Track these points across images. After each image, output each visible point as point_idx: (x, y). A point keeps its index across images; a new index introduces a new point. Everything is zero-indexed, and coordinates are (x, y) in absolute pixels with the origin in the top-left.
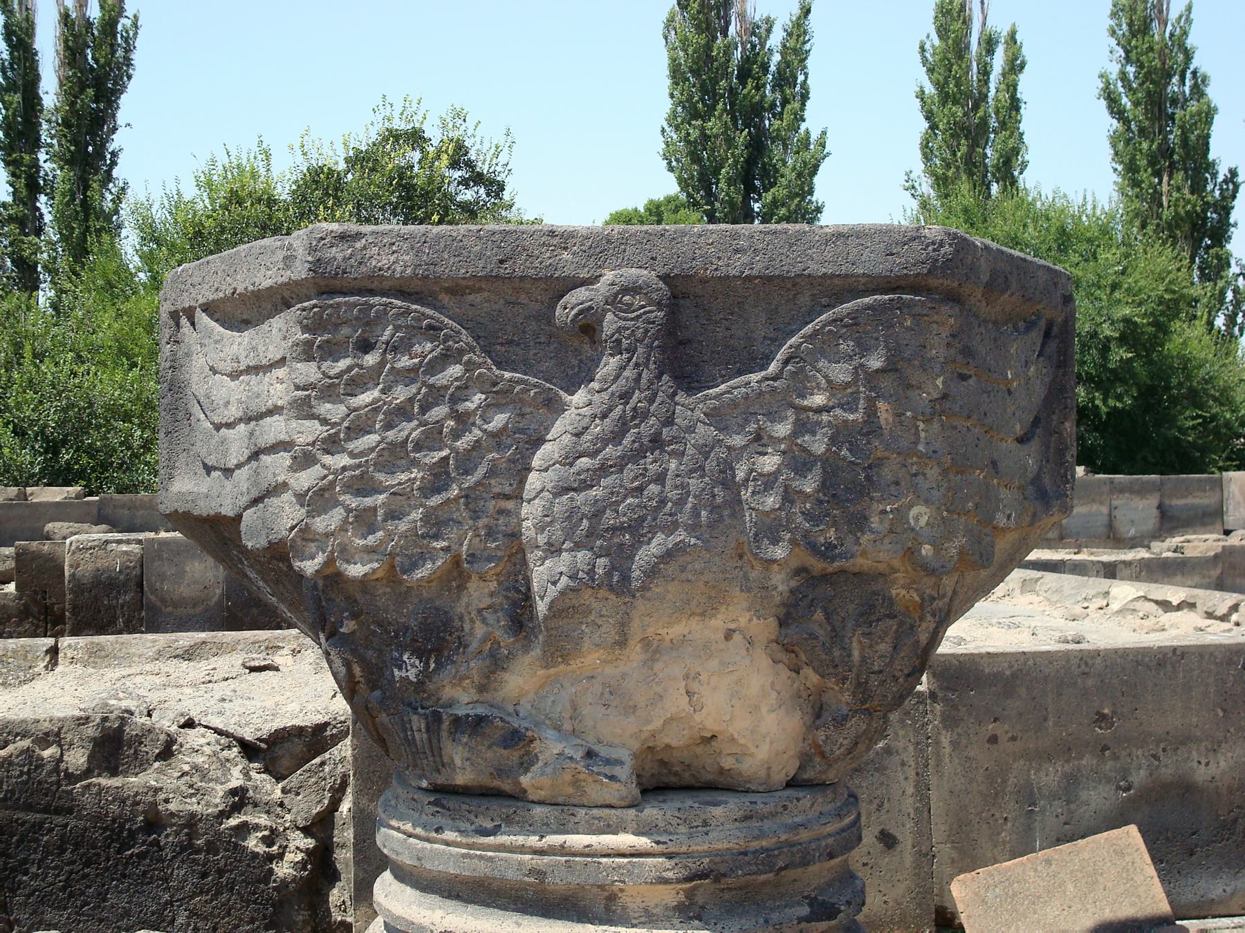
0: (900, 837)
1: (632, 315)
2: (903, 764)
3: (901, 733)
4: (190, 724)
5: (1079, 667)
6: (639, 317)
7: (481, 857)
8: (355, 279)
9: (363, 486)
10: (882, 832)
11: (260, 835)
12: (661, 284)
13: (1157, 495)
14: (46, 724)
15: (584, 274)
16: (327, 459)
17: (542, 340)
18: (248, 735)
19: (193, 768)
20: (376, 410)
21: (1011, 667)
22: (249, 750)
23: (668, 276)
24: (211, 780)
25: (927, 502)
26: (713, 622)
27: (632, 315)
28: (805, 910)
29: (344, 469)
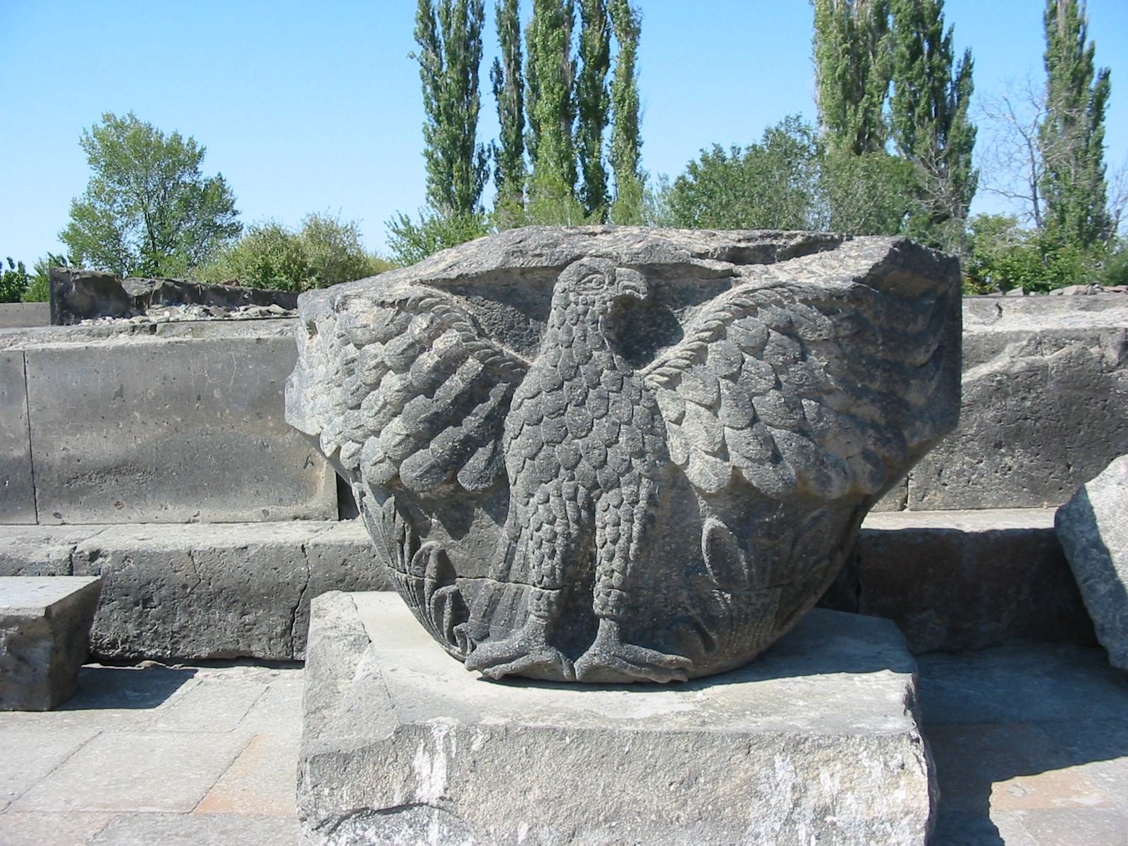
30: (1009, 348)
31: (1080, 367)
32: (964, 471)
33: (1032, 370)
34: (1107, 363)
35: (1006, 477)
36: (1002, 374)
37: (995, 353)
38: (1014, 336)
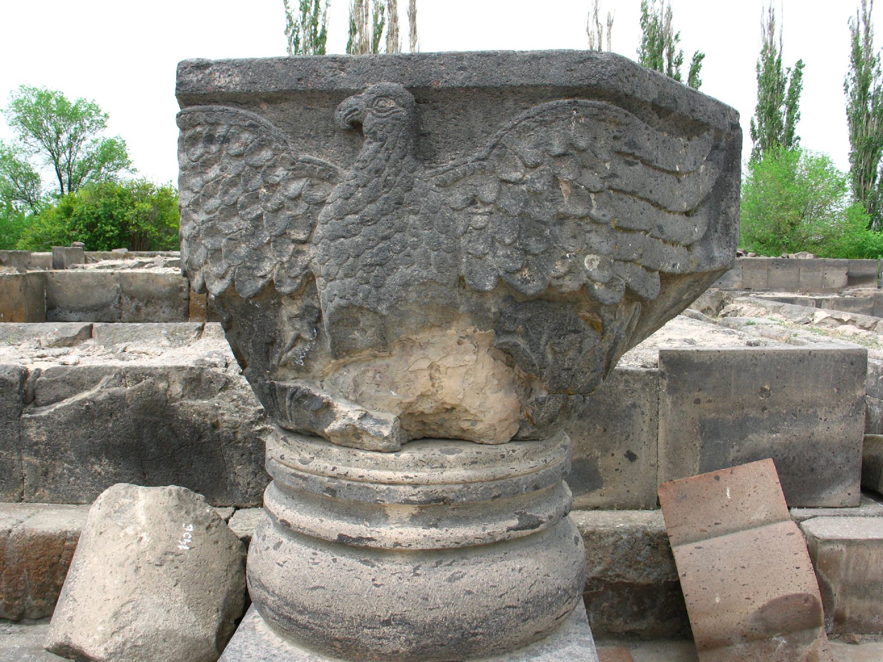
0: (638, 455)
1: (385, 115)
2: (643, 413)
5: (752, 360)
6: (387, 116)
7: (301, 477)
8: (205, 94)
9: (212, 231)
10: (628, 452)
12: (407, 93)
13: (846, 268)
14: (160, 370)
16: (195, 216)
17: (329, 134)
19: (239, 397)
20: (218, 182)
21: (710, 359)
23: (412, 87)
24: (249, 404)
25: (597, 252)
26: (449, 331)
27: (385, 115)
28: (515, 522)
29: (203, 222)
30: (103, 381)
31: (150, 398)
32: (64, 474)
33: (113, 398)
34: (170, 395)
35: (96, 480)
36: (89, 401)
37: (95, 382)
38: (108, 371)
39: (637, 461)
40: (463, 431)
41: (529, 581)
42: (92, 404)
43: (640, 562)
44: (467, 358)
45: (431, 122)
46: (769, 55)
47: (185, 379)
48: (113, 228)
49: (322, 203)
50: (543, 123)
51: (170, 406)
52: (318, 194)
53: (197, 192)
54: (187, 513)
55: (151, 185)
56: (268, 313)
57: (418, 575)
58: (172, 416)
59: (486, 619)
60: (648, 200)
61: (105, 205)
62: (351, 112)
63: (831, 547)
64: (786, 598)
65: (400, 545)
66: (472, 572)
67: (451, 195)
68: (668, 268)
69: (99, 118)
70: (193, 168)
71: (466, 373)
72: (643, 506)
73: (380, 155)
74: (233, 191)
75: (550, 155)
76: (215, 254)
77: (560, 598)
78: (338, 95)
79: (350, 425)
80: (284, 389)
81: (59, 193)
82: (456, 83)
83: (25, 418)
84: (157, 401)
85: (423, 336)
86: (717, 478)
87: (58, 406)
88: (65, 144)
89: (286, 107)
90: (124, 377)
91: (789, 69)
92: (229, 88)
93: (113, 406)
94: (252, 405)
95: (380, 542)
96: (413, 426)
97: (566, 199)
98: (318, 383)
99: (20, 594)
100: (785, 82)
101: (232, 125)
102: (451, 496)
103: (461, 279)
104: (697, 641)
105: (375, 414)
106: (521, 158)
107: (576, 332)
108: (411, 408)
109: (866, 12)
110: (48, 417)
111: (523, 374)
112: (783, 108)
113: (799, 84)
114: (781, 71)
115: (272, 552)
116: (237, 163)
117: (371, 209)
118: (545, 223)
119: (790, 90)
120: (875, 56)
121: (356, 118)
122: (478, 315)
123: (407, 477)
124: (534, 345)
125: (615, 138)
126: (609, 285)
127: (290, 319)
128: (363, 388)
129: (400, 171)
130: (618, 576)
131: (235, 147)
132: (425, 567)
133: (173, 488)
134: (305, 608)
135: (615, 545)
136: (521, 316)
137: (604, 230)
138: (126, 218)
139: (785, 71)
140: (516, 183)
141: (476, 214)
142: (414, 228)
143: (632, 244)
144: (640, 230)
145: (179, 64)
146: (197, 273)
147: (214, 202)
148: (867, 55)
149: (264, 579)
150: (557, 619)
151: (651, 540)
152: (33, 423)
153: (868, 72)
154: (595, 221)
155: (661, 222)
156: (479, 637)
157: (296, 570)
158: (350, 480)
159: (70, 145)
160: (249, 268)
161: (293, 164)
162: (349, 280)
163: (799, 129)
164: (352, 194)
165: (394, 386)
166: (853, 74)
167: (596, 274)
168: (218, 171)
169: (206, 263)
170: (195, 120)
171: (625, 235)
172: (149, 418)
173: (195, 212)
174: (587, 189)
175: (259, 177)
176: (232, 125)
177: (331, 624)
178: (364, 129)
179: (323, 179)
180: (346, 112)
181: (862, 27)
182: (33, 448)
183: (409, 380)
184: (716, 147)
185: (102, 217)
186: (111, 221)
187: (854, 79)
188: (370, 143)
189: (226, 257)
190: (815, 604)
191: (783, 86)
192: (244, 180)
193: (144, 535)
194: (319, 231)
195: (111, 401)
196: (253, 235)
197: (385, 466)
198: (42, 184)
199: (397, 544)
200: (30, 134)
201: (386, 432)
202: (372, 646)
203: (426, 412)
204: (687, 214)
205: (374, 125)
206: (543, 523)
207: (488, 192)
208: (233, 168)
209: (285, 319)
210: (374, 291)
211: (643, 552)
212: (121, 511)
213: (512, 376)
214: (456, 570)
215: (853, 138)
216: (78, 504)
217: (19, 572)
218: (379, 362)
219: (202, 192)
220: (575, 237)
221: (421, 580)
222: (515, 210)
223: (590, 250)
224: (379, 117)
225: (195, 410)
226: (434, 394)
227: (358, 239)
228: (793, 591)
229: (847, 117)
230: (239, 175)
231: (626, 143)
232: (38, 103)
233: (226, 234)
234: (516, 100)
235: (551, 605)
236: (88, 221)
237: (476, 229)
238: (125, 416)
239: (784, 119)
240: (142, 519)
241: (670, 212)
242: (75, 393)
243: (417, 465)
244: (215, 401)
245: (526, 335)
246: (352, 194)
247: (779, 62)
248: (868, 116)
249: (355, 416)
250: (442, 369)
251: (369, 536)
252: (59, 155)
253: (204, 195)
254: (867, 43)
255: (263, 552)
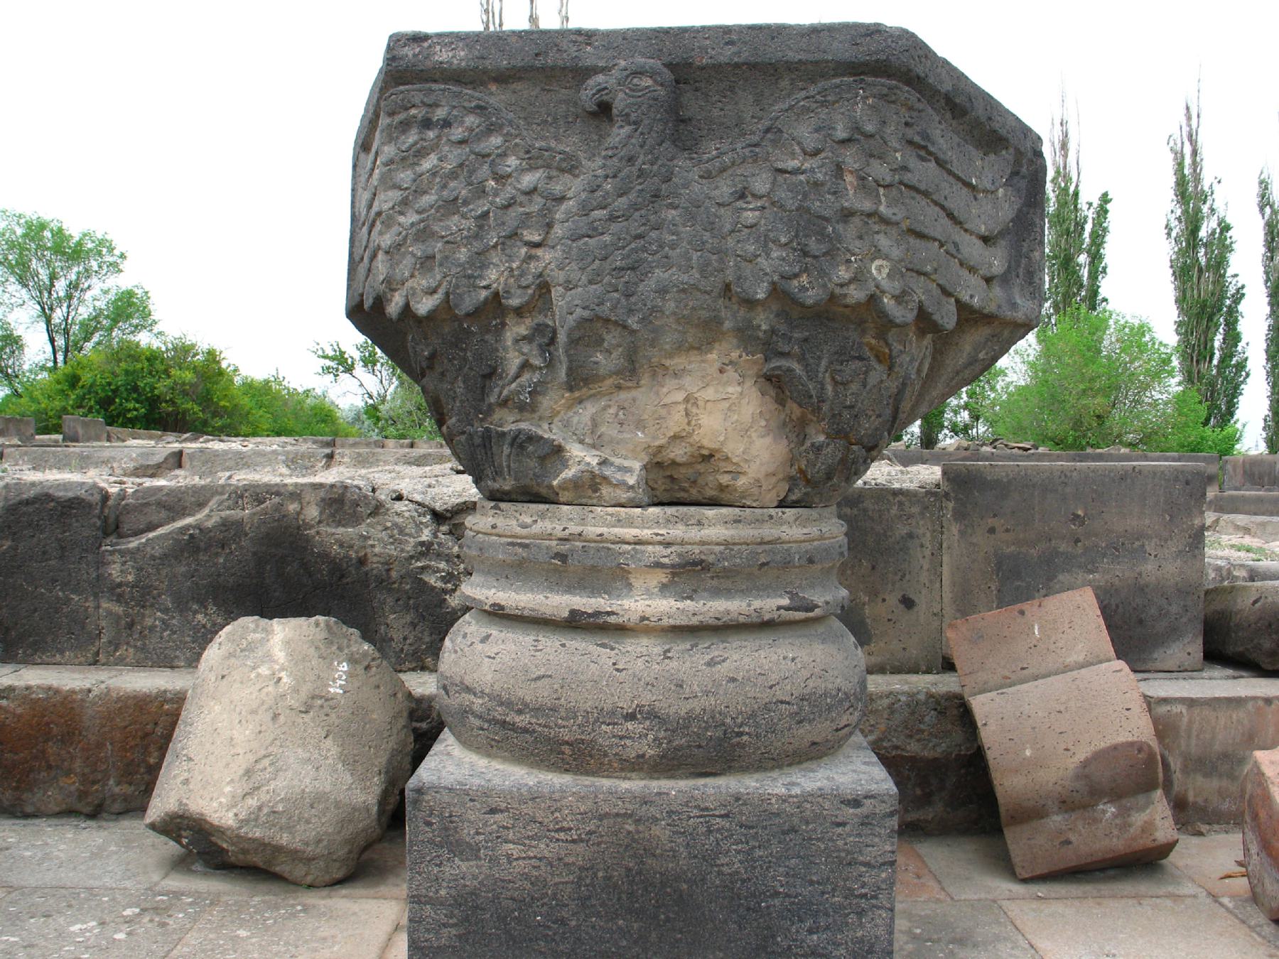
0: (917, 601)
1: (640, 94)
2: (922, 546)
3: (921, 523)
4: (399, 498)
6: (643, 95)
7: (520, 545)
8: (422, 71)
9: (423, 234)
10: (904, 596)
11: (438, 575)
12: (665, 70)
14: (291, 488)
15: (601, 64)
16: (402, 219)
17: (570, 120)
18: (438, 506)
20: (434, 174)
21: (1007, 475)
22: (439, 517)
23: (671, 64)
24: (407, 535)
25: (887, 258)
26: (709, 356)
27: (640, 94)
28: (785, 601)
29: (413, 224)
31: (276, 524)
32: (156, 626)
33: (225, 524)
34: (303, 520)
36: (194, 527)
37: (201, 505)
38: (219, 490)
39: (916, 609)
40: (722, 488)
41: (806, 673)
42: (198, 531)
43: (923, 731)
44: (730, 389)
45: (692, 105)
46: (1063, 185)
47: (323, 500)
48: (137, 405)
49: (561, 199)
50: (823, 104)
51: (302, 534)
52: (557, 188)
53: (406, 189)
54: (340, 649)
55: (193, 346)
56: (487, 337)
57: (669, 658)
58: (305, 549)
59: (753, 715)
60: (943, 207)
61: (127, 372)
62: (599, 91)
63: (1169, 708)
64: (1115, 748)
65: (648, 619)
66: (735, 657)
67: (717, 187)
68: (965, 297)
69: (111, 259)
70: (403, 159)
71: (729, 409)
72: (924, 668)
73: (633, 141)
74: (452, 184)
75: (834, 141)
76: (426, 262)
77: (841, 701)
78: (581, 73)
79: (588, 471)
80: (503, 434)
81: (50, 364)
82: (722, 59)
83: (107, 551)
84: (286, 528)
85: (678, 362)
86: (1022, 613)
87: (151, 535)
88: (62, 294)
89: (519, 88)
90: (242, 497)
91: (1090, 204)
92: (451, 64)
93: (226, 534)
94: (410, 535)
95: (623, 616)
96: (659, 482)
97: (851, 192)
98: (546, 426)
99: (99, 776)
100: (1086, 222)
101: (455, 107)
102: (711, 559)
103: (727, 287)
104: (1002, 810)
105: (617, 461)
106: (799, 143)
107: (860, 358)
108: (660, 456)
109: (1191, 129)
110: (138, 549)
111: (797, 411)
112: (1083, 258)
113: (1105, 225)
114: (1079, 206)
115: (479, 647)
116: (459, 151)
117: (622, 203)
118: (827, 220)
119: (1091, 235)
120: (1206, 188)
121: (605, 98)
122: (746, 335)
123: (657, 534)
124: (812, 374)
125: (907, 124)
126: (899, 298)
127: (517, 341)
128: (603, 429)
129: (657, 158)
130: (897, 748)
131: (457, 133)
132: (680, 646)
133: (321, 618)
134: (526, 705)
135: (891, 709)
136: (797, 335)
137: (894, 231)
138: (156, 392)
139: (1085, 207)
140: (797, 171)
141: (746, 209)
142: (674, 225)
143: (927, 254)
144: (935, 240)
145: (391, 37)
146: (397, 294)
147: (427, 200)
148: (1196, 187)
149: (468, 680)
150: (837, 730)
151: (938, 703)
152: (117, 557)
153: (1198, 211)
154: (885, 221)
155: (957, 239)
156: (745, 738)
157: (514, 660)
158: (585, 541)
159: (69, 297)
160: (470, 277)
161: (528, 152)
162: (594, 287)
163: (1106, 287)
164: (599, 186)
165: (641, 425)
166: (1179, 212)
167: (885, 284)
168: (435, 162)
169: (412, 276)
170: (410, 102)
171: (918, 241)
172: (273, 550)
173: (401, 213)
174: (876, 181)
175: (486, 167)
176: (455, 107)
177: (560, 721)
178: (615, 111)
179: (562, 171)
180: (594, 91)
181: (1188, 150)
182: (116, 591)
183: (660, 418)
184: (1015, 173)
185: (122, 389)
186: (135, 396)
187: (1179, 219)
188: (622, 127)
189: (441, 265)
190: (1151, 755)
191: (1083, 229)
192: (468, 171)
193: (283, 674)
194: (558, 231)
195: (224, 529)
196: (476, 237)
197: (630, 523)
198: (26, 350)
199: (643, 618)
200: (12, 279)
201: (631, 481)
202: (611, 746)
203: (679, 460)
204: (986, 240)
205: (627, 106)
206: (819, 607)
207: (761, 184)
208: (454, 157)
209: (509, 343)
210: (623, 300)
211: (927, 719)
212: (251, 648)
213: (783, 416)
214: (716, 653)
215: (1180, 301)
216: (172, 667)
217: (100, 745)
218: (623, 395)
219: (413, 188)
220: (860, 237)
221: (674, 664)
222: (791, 204)
223: (878, 253)
224: (633, 97)
225: (337, 541)
226: (690, 435)
227: (607, 238)
228: (1123, 738)
229: (1171, 271)
230: (461, 165)
231: (918, 133)
232: (25, 236)
233: (443, 237)
234: (793, 79)
235: (829, 709)
236: (102, 395)
237: (747, 227)
238: (241, 548)
239: (1085, 273)
240: (280, 655)
241: (966, 230)
242: (174, 520)
243: (668, 521)
244: (363, 529)
245: (802, 359)
246: (599, 186)
247: (1076, 194)
248: (1200, 270)
249: (594, 462)
250: (701, 403)
251: (609, 609)
252: (51, 309)
253: (415, 191)
254: (1195, 170)
255: (466, 649)
